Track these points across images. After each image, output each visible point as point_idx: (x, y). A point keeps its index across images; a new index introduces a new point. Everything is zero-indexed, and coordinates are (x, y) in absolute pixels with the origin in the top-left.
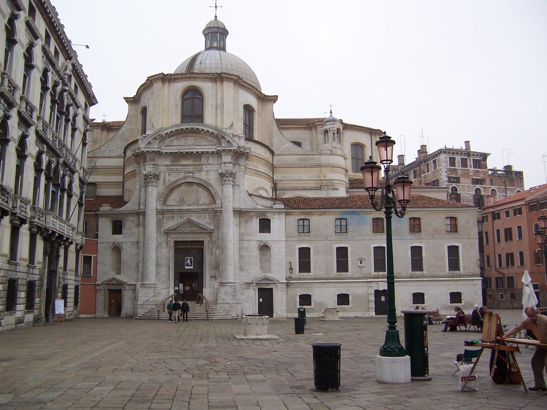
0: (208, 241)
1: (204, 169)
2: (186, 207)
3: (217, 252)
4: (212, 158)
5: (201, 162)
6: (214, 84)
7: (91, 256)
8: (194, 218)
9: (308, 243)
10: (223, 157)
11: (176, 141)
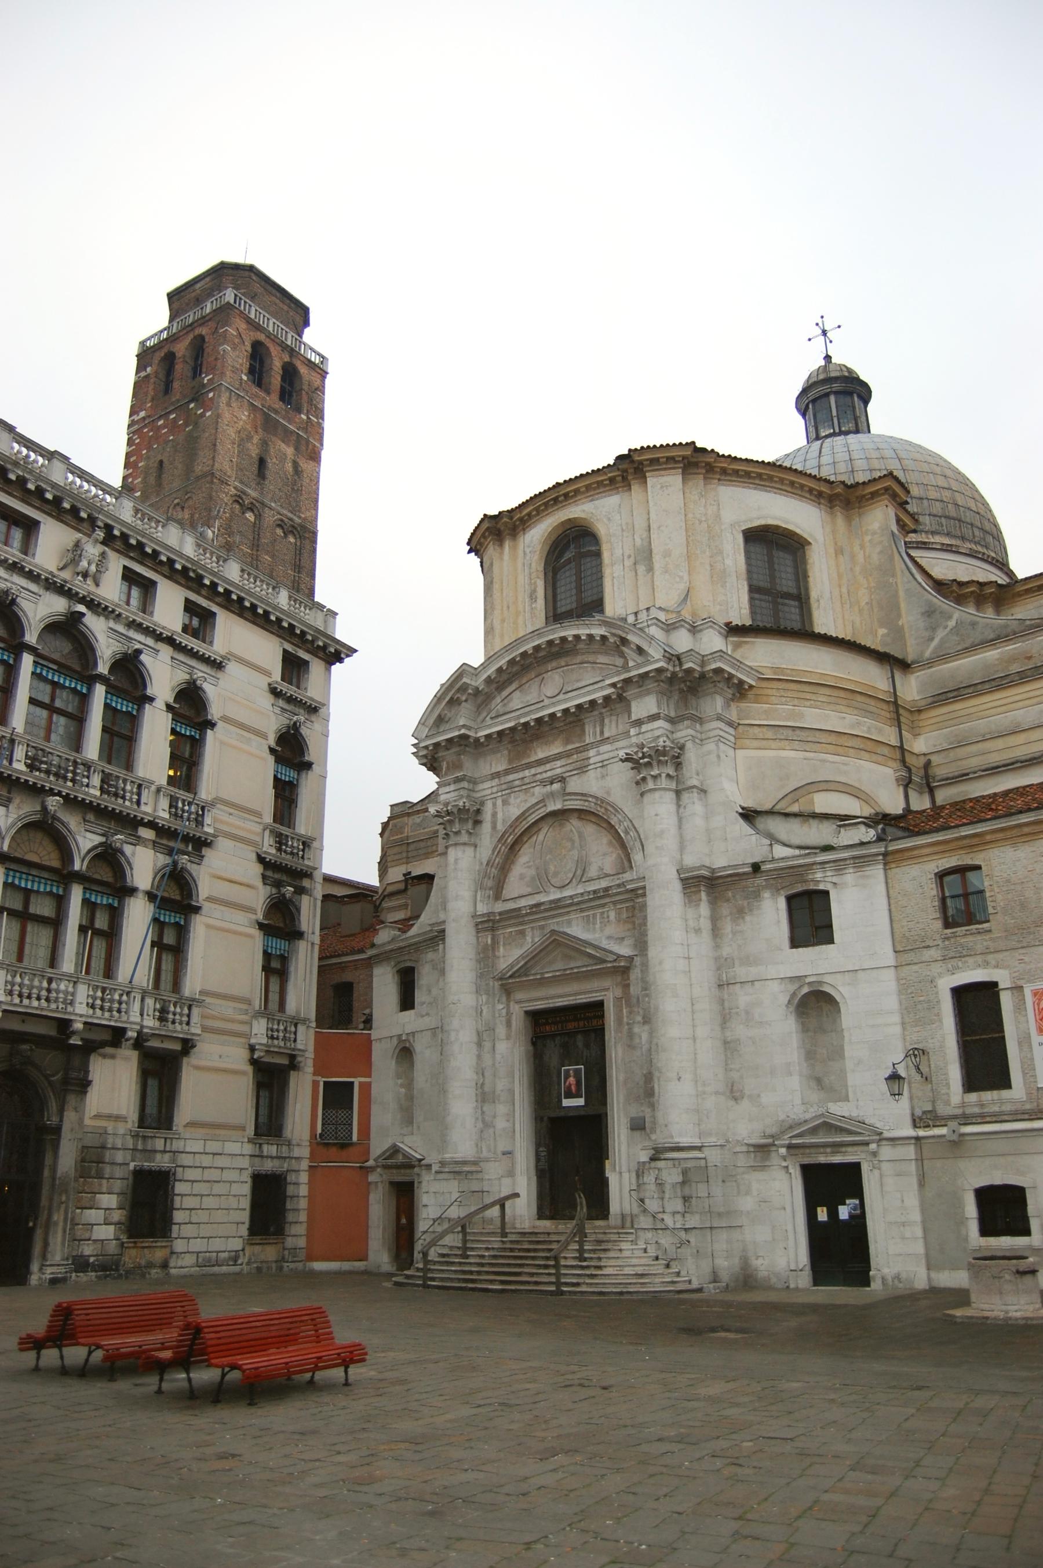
0: (618, 1000)
1: (592, 761)
2: (555, 895)
3: (645, 1036)
4: (614, 718)
5: (585, 741)
6: (627, 494)
7: (352, 1083)
8: (577, 929)
9: (986, 964)
10: (634, 705)
11: (517, 693)
